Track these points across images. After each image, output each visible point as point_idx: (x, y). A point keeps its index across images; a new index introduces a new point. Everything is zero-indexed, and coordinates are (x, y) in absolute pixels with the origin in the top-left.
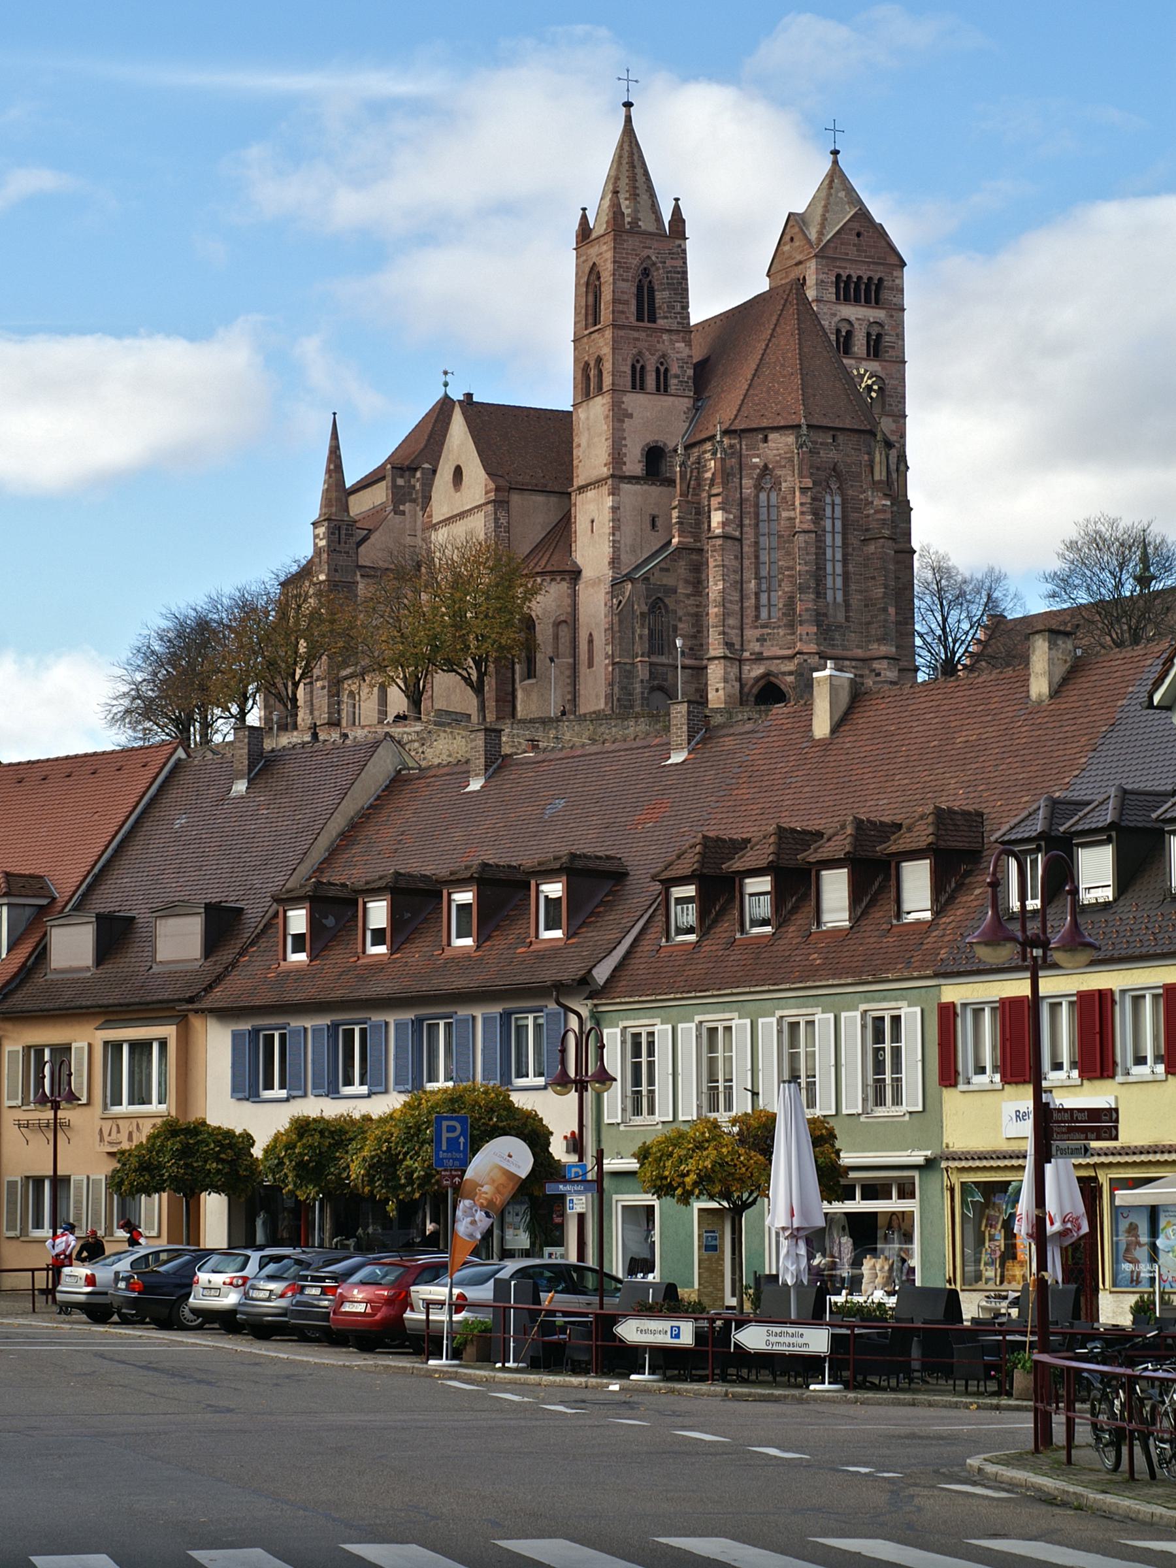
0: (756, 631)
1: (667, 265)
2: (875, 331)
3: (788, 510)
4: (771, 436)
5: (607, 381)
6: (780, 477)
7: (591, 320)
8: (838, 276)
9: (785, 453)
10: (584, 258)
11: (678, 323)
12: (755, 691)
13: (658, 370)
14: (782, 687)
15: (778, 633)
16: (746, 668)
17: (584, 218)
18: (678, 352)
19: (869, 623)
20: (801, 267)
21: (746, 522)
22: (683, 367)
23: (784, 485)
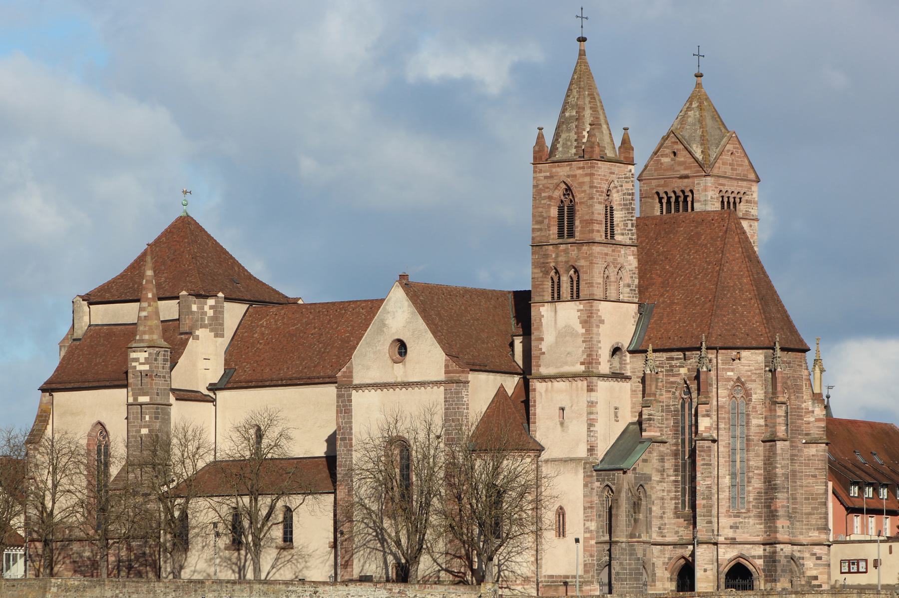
0: (729, 519)
1: (624, 188)
3: (758, 418)
4: (745, 354)
6: (751, 389)
7: (554, 230)
8: (721, 191)
9: (755, 369)
10: (548, 174)
11: (630, 239)
12: (726, 570)
14: (751, 567)
15: (749, 522)
16: (722, 549)
17: (540, 138)
18: (630, 264)
19: (810, 514)
20: (686, 180)
21: (722, 426)
22: (632, 277)
23: (754, 397)
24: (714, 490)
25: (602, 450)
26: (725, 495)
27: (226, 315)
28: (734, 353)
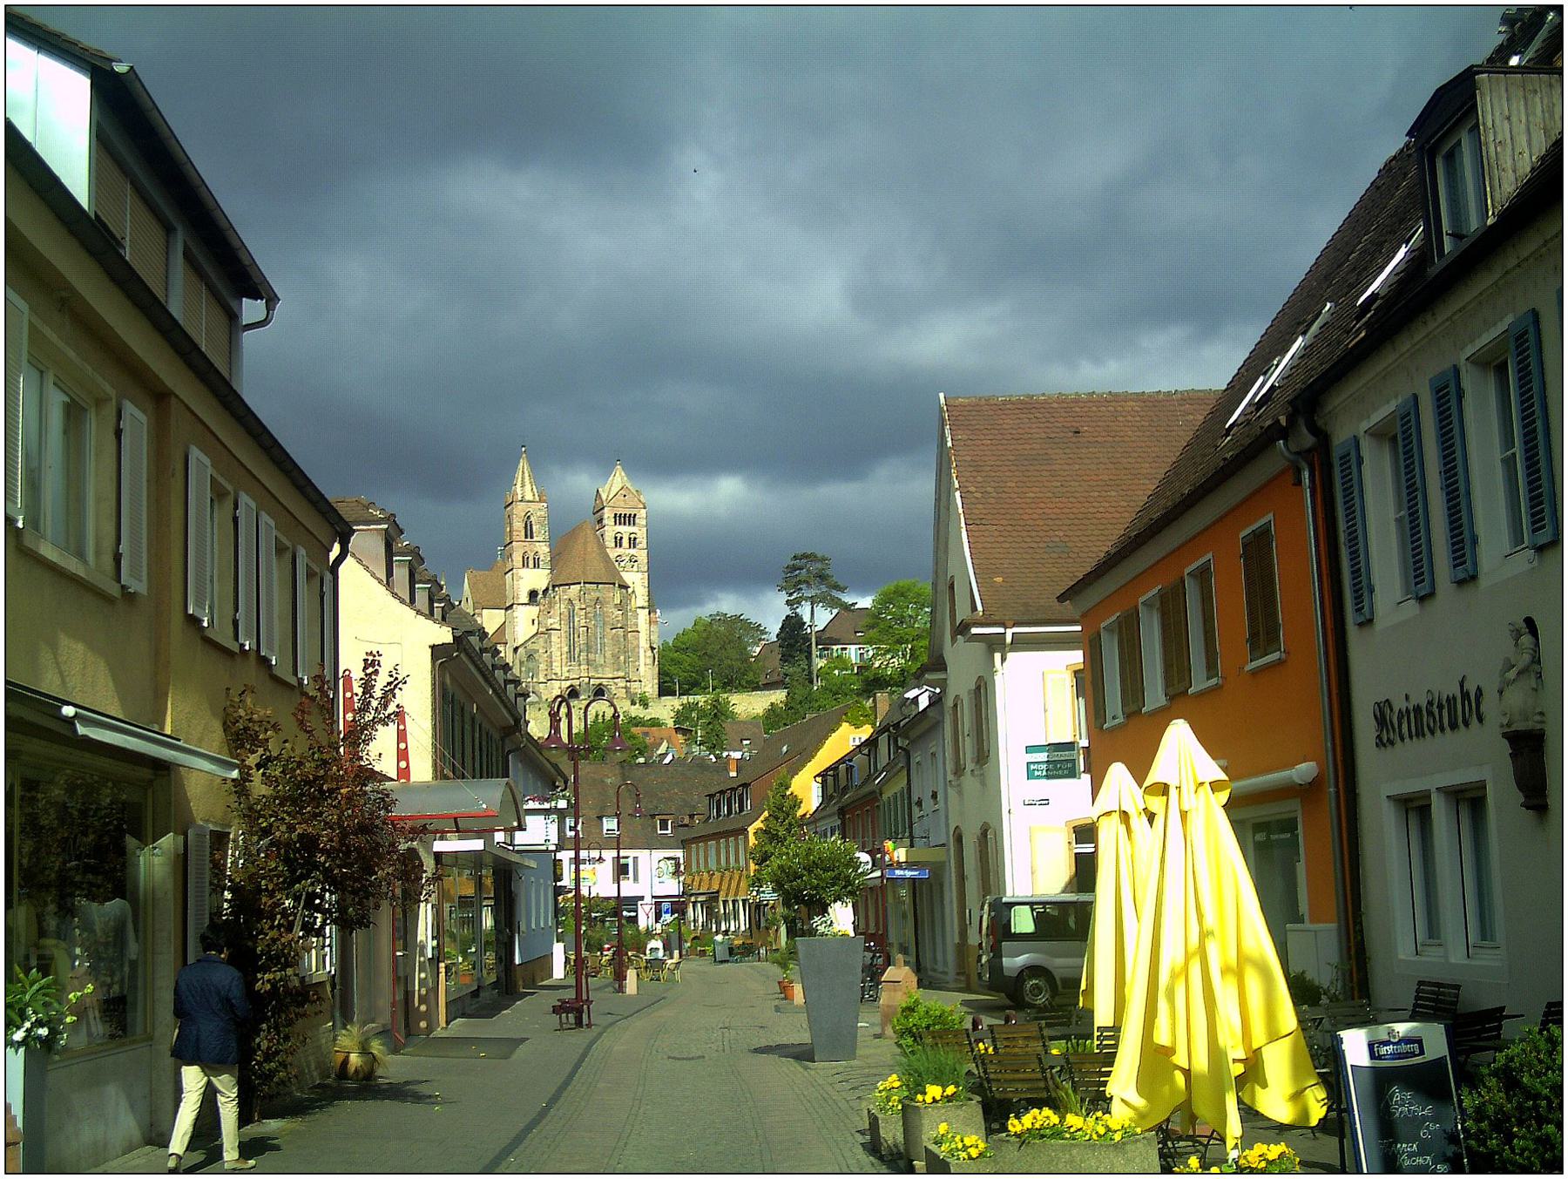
2: (632, 536)
4: (572, 587)
8: (616, 514)
13: (534, 558)
21: (562, 622)
28: (567, 587)
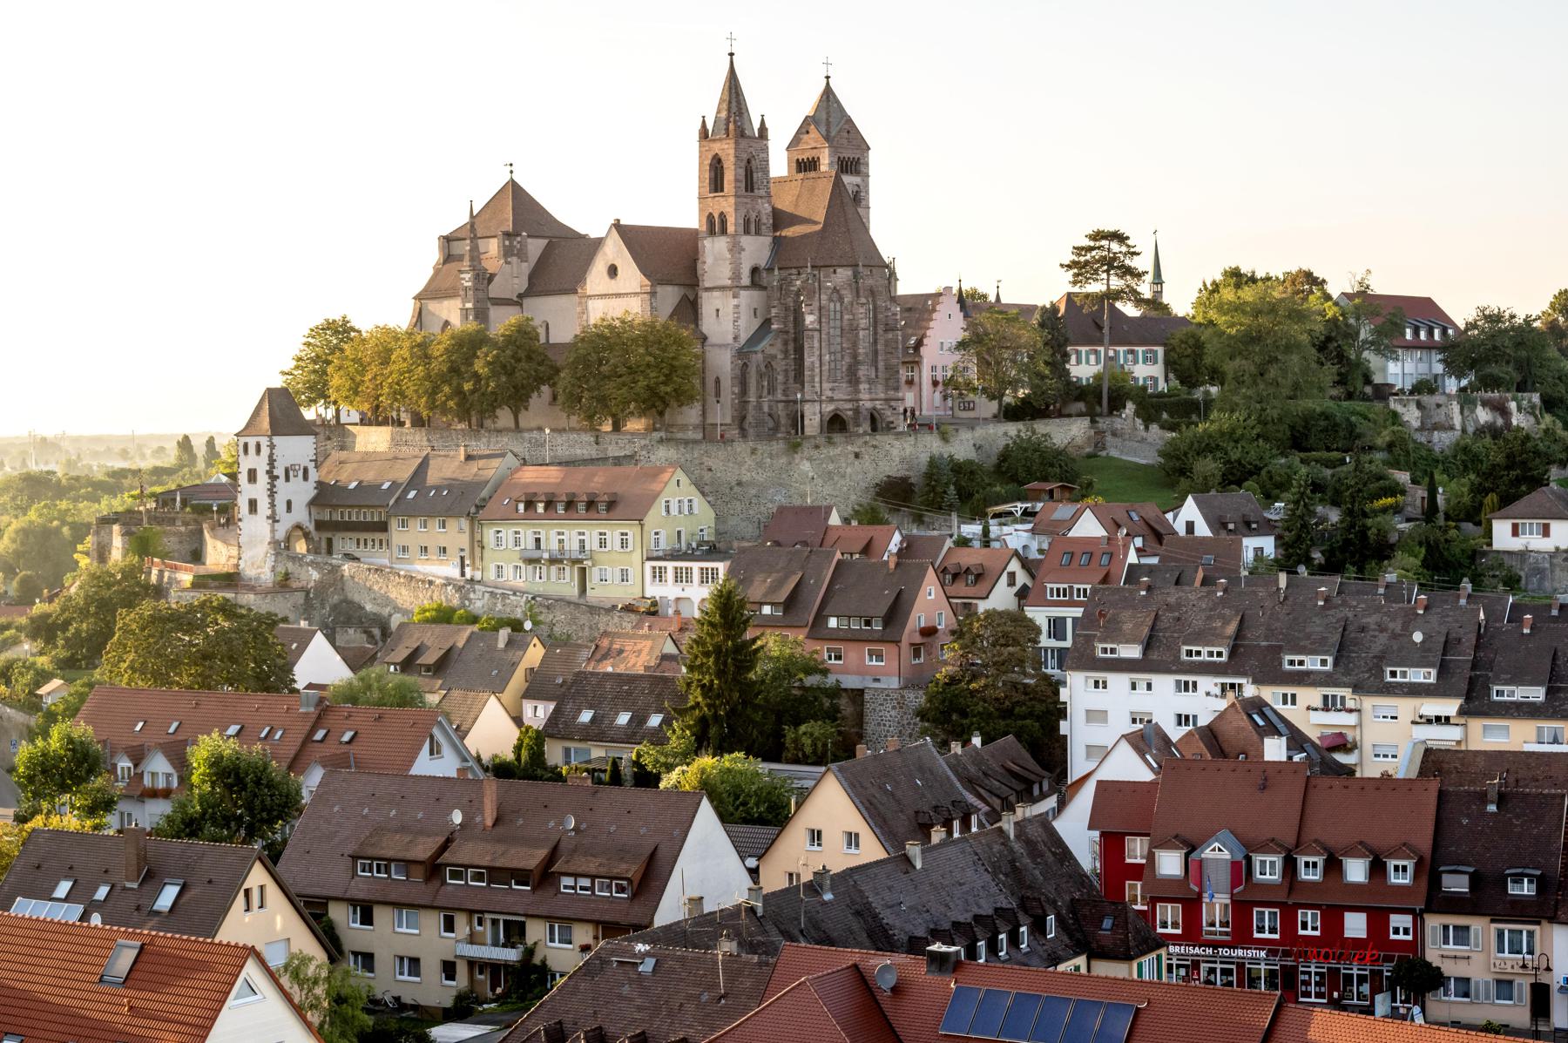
2: (856, 189)
4: (839, 270)
5: (731, 229)
17: (704, 122)
24: (817, 365)
25: (744, 338)
26: (825, 368)
27: (529, 247)
